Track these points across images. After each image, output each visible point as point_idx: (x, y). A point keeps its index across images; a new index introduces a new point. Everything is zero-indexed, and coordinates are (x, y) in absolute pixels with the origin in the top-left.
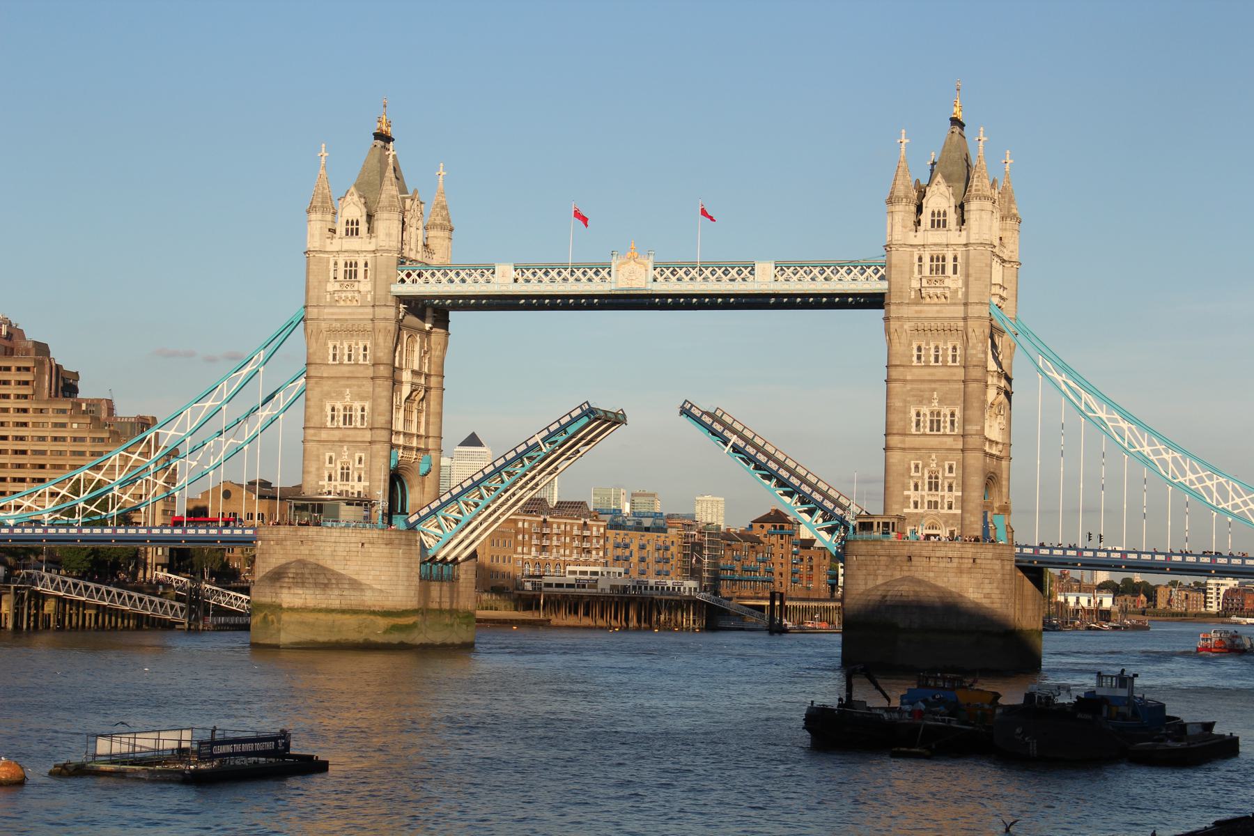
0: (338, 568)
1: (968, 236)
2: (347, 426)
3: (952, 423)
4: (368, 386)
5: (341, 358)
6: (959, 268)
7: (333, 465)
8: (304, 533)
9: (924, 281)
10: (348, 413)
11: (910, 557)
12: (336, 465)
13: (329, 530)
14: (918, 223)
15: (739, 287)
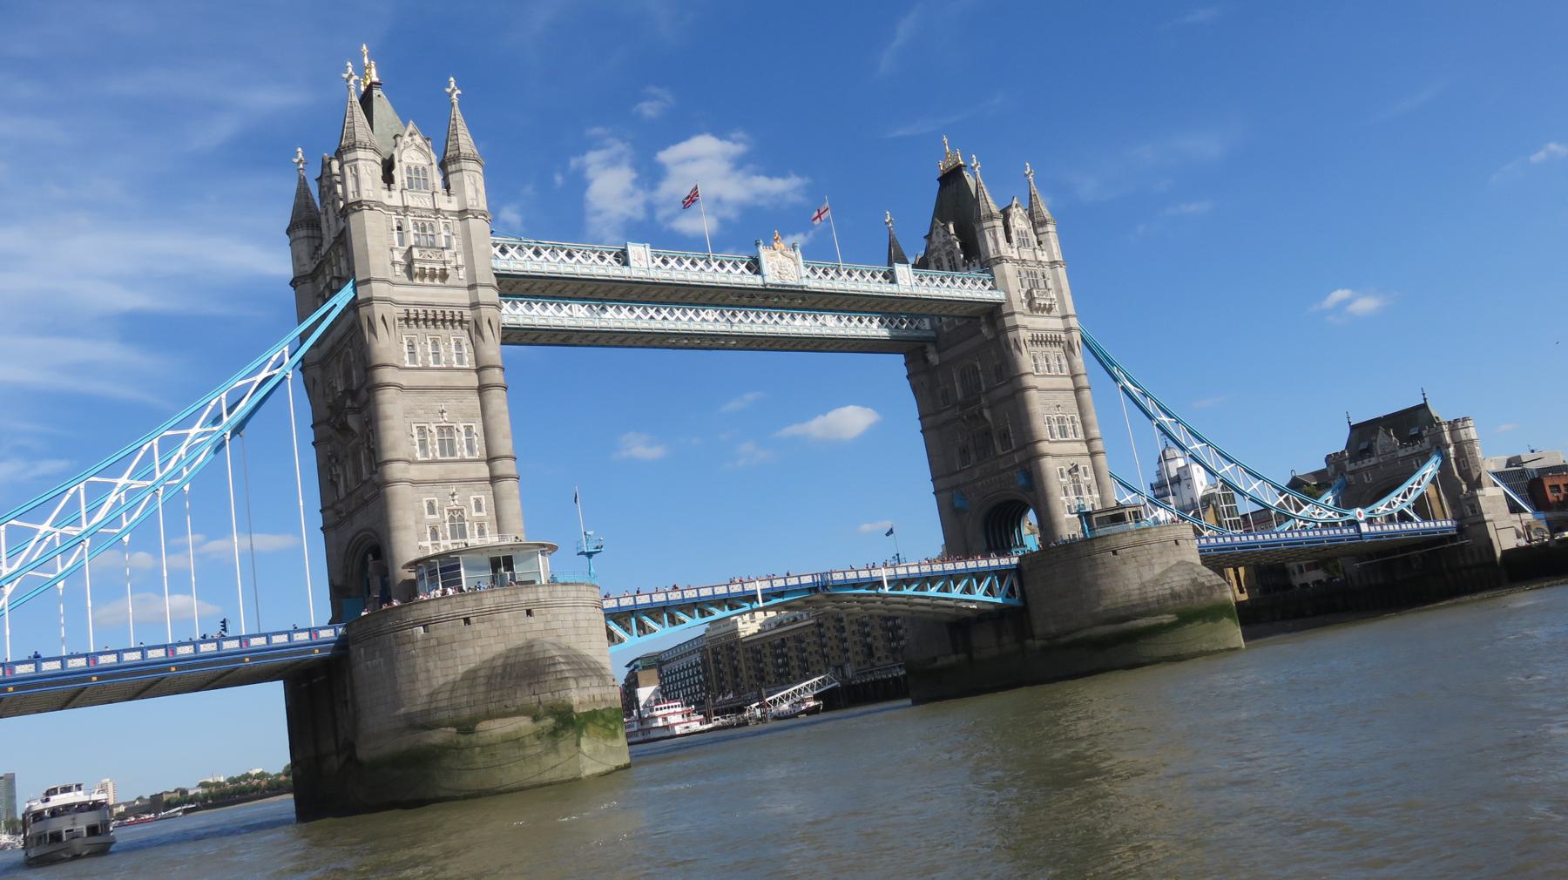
1: (1050, 254)
3: (1073, 426)
5: (425, 359)
7: (438, 516)
8: (532, 596)
9: (1035, 291)
12: (442, 515)
13: (564, 588)
14: (1009, 240)
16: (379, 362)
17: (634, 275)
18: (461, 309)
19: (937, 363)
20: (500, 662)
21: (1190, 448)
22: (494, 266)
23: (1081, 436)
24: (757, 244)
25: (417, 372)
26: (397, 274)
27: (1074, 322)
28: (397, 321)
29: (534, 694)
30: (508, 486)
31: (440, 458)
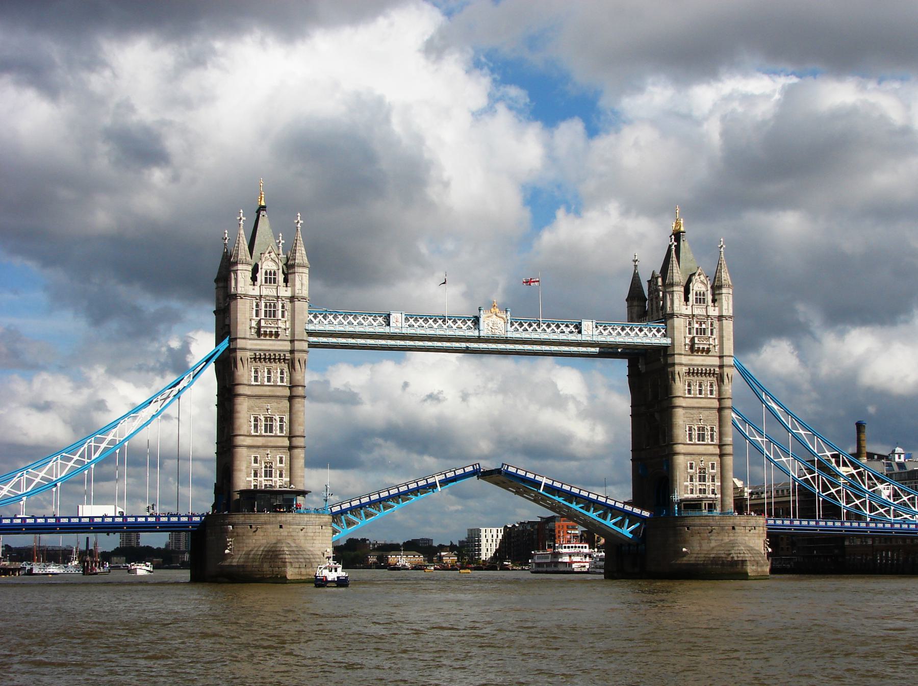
0: (308, 546)
1: (721, 310)
2: (268, 434)
3: (712, 435)
4: (286, 403)
5: (263, 380)
6: (715, 331)
7: (258, 465)
8: (283, 519)
9: (696, 339)
10: (269, 423)
11: (733, 528)
12: (261, 464)
13: (302, 516)
14: (687, 299)
15: (572, 337)
16: (237, 382)
17: (391, 332)
18: (285, 353)
19: (643, 372)
20: (262, 549)
21: (819, 455)
22: (307, 328)
23: (716, 441)
24: (480, 310)
25: (257, 387)
26: (252, 333)
27: (729, 361)
28: (249, 360)
29: (271, 567)
30: (296, 451)
31: (264, 434)
